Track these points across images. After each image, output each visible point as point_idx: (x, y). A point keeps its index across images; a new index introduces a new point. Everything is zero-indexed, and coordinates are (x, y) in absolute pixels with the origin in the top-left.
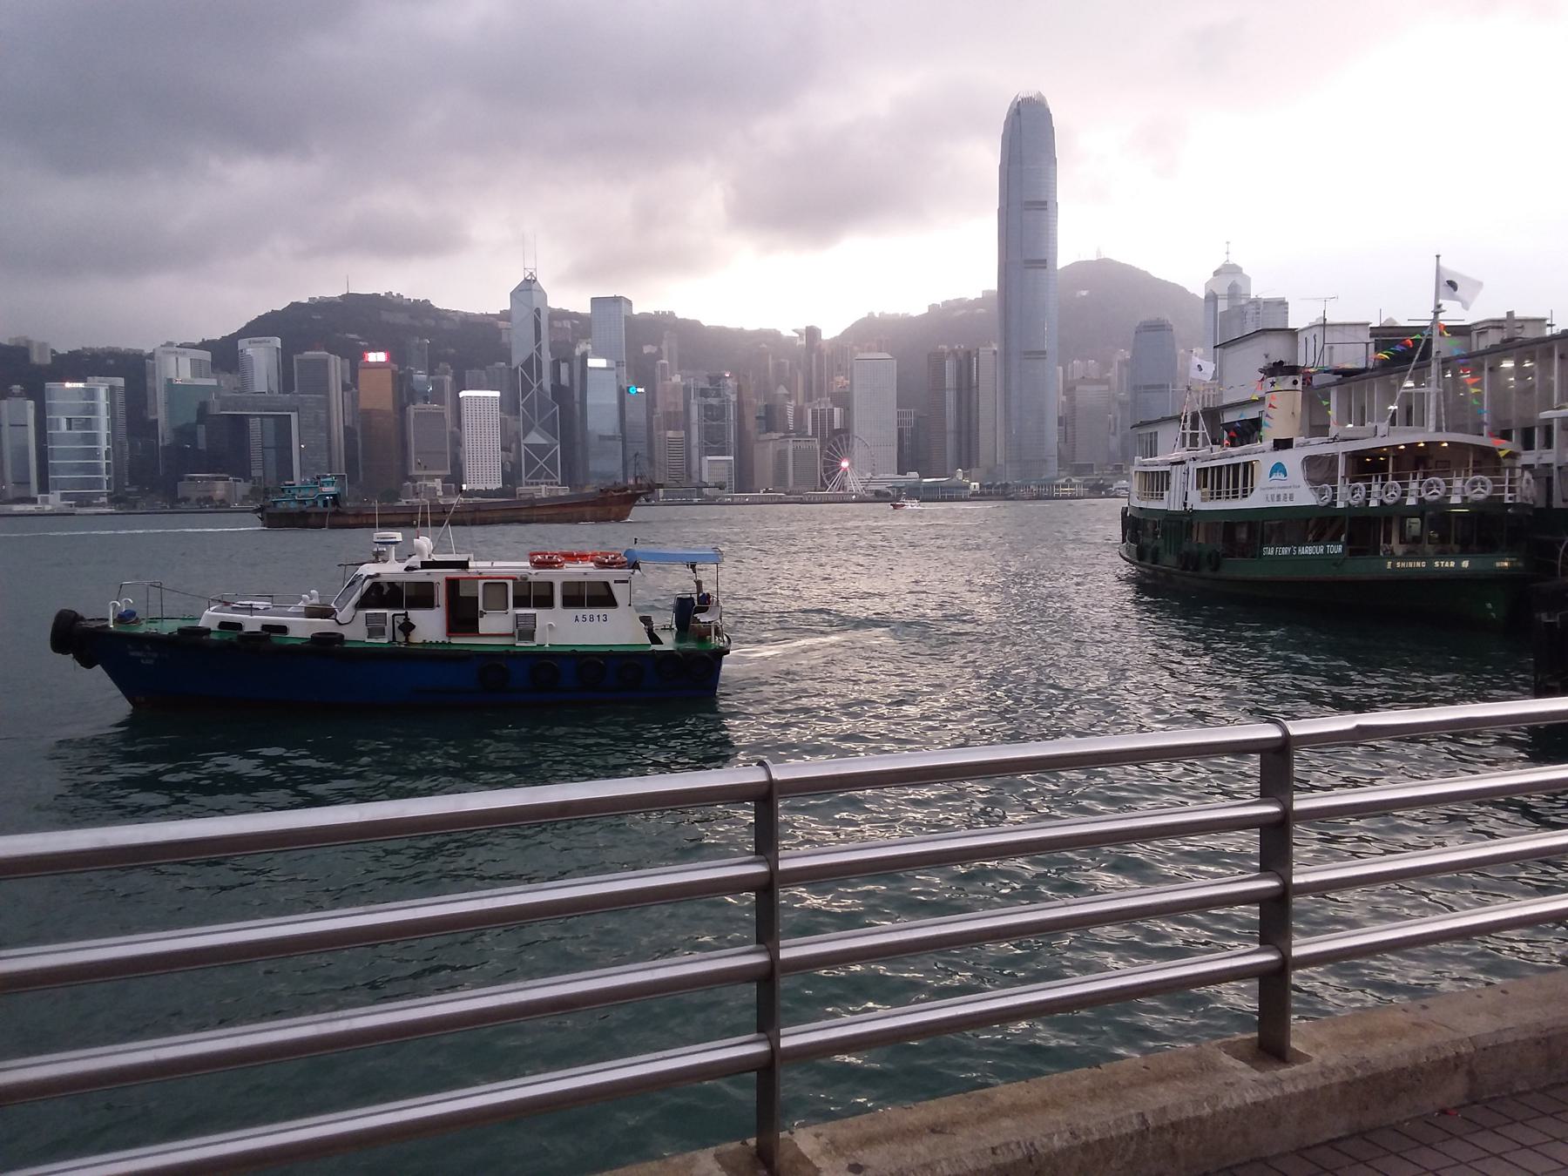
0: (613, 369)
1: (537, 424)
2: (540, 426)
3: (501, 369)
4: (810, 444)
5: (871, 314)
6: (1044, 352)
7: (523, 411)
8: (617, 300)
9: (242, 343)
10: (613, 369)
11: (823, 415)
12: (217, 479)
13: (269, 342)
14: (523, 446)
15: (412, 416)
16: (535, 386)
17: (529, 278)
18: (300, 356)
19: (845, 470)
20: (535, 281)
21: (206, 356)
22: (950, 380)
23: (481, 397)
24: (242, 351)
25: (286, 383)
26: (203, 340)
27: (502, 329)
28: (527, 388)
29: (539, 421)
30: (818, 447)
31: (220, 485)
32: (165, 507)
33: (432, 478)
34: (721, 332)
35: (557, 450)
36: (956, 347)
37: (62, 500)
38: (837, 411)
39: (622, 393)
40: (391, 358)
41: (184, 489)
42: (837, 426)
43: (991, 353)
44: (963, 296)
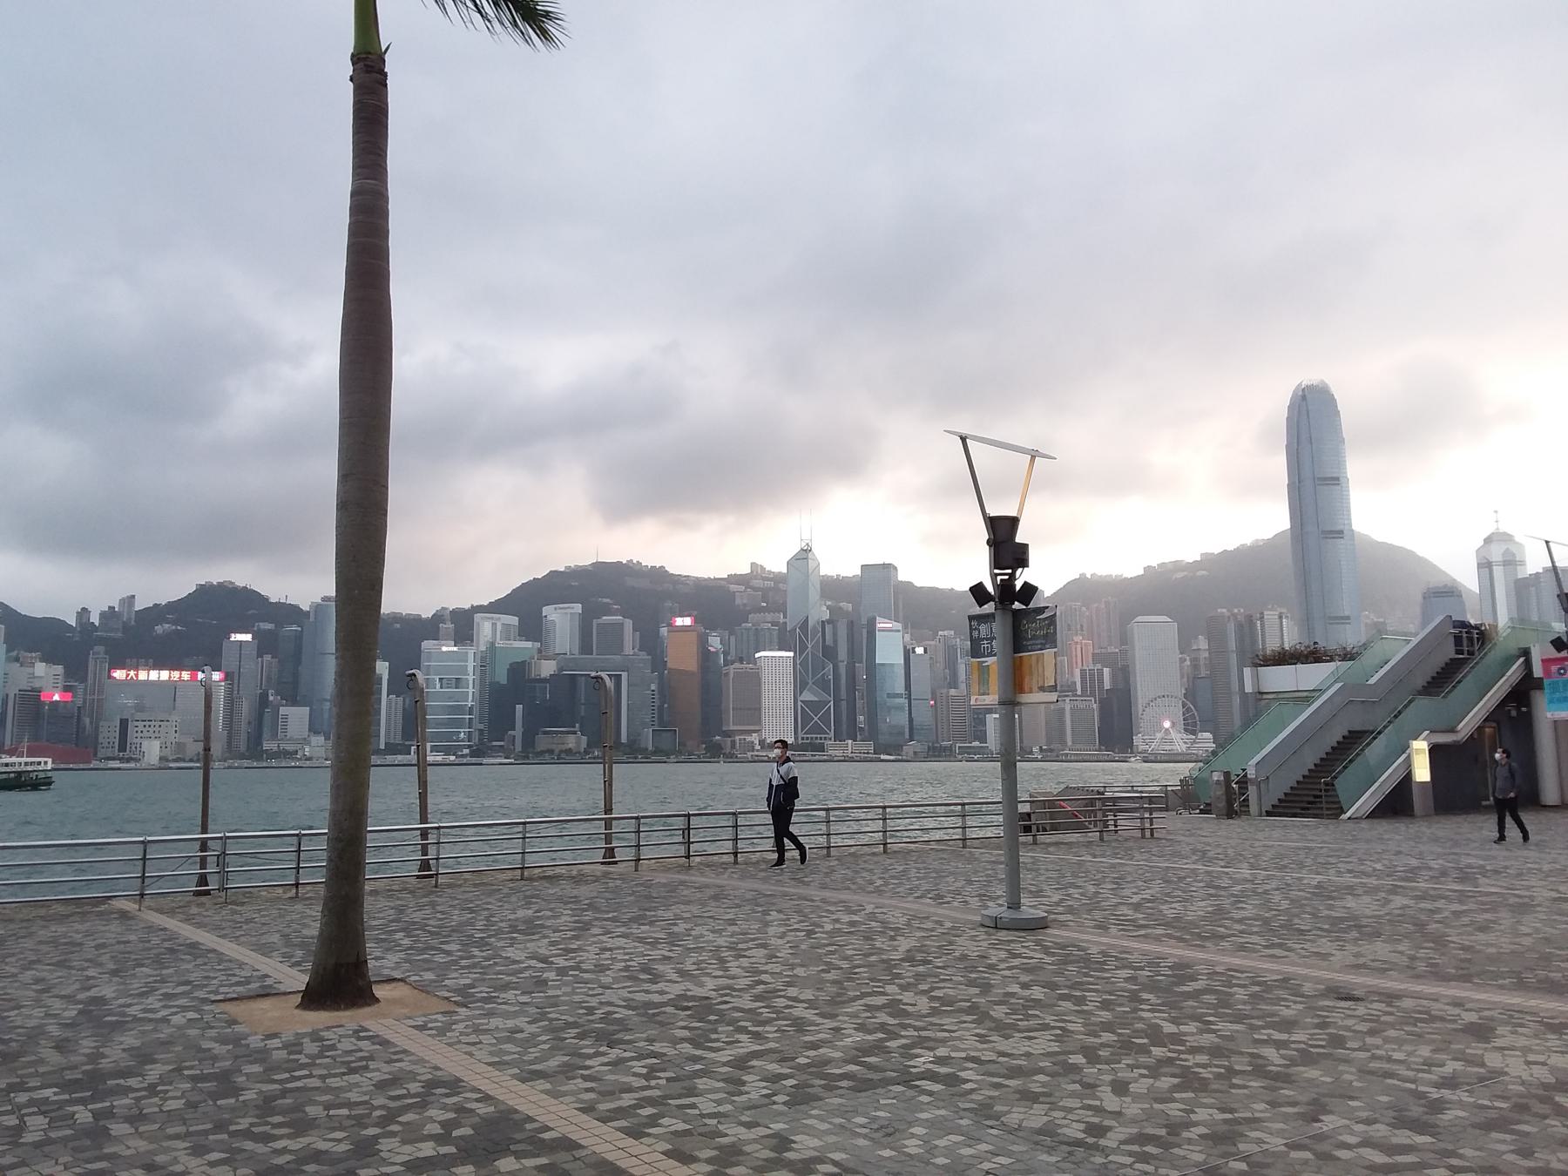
0: (899, 631)
1: (811, 683)
2: (813, 683)
3: (748, 630)
4: (1087, 703)
5: (1083, 575)
6: (1348, 618)
7: (800, 672)
8: (888, 569)
9: (546, 610)
10: (899, 631)
11: (1092, 675)
12: (568, 733)
13: (573, 608)
14: (799, 703)
15: (731, 676)
16: (810, 646)
17: (805, 548)
18: (600, 621)
19: (1167, 730)
20: (810, 550)
21: (514, 620)
22: (1232, 645)
23: (776, 660)
24: (546, 617)
25: (586, 648)
26: (472, 606)
27: (734, 592)
28: (803, 648)
29: (812, 679)
30: (1095, 706)
31: (572, 737)
32: (553, 758)
33: (750, 732)
34: (933, 591)
35: (830, 706)
36: (1236, 611)
37: (431, 752)
38: (1106, 671)
39: (908, 653)
40: (696, 621)
41: (542, 742)
42: (1107, 686)
43: (1277, 617)
44: (1168, 557)
